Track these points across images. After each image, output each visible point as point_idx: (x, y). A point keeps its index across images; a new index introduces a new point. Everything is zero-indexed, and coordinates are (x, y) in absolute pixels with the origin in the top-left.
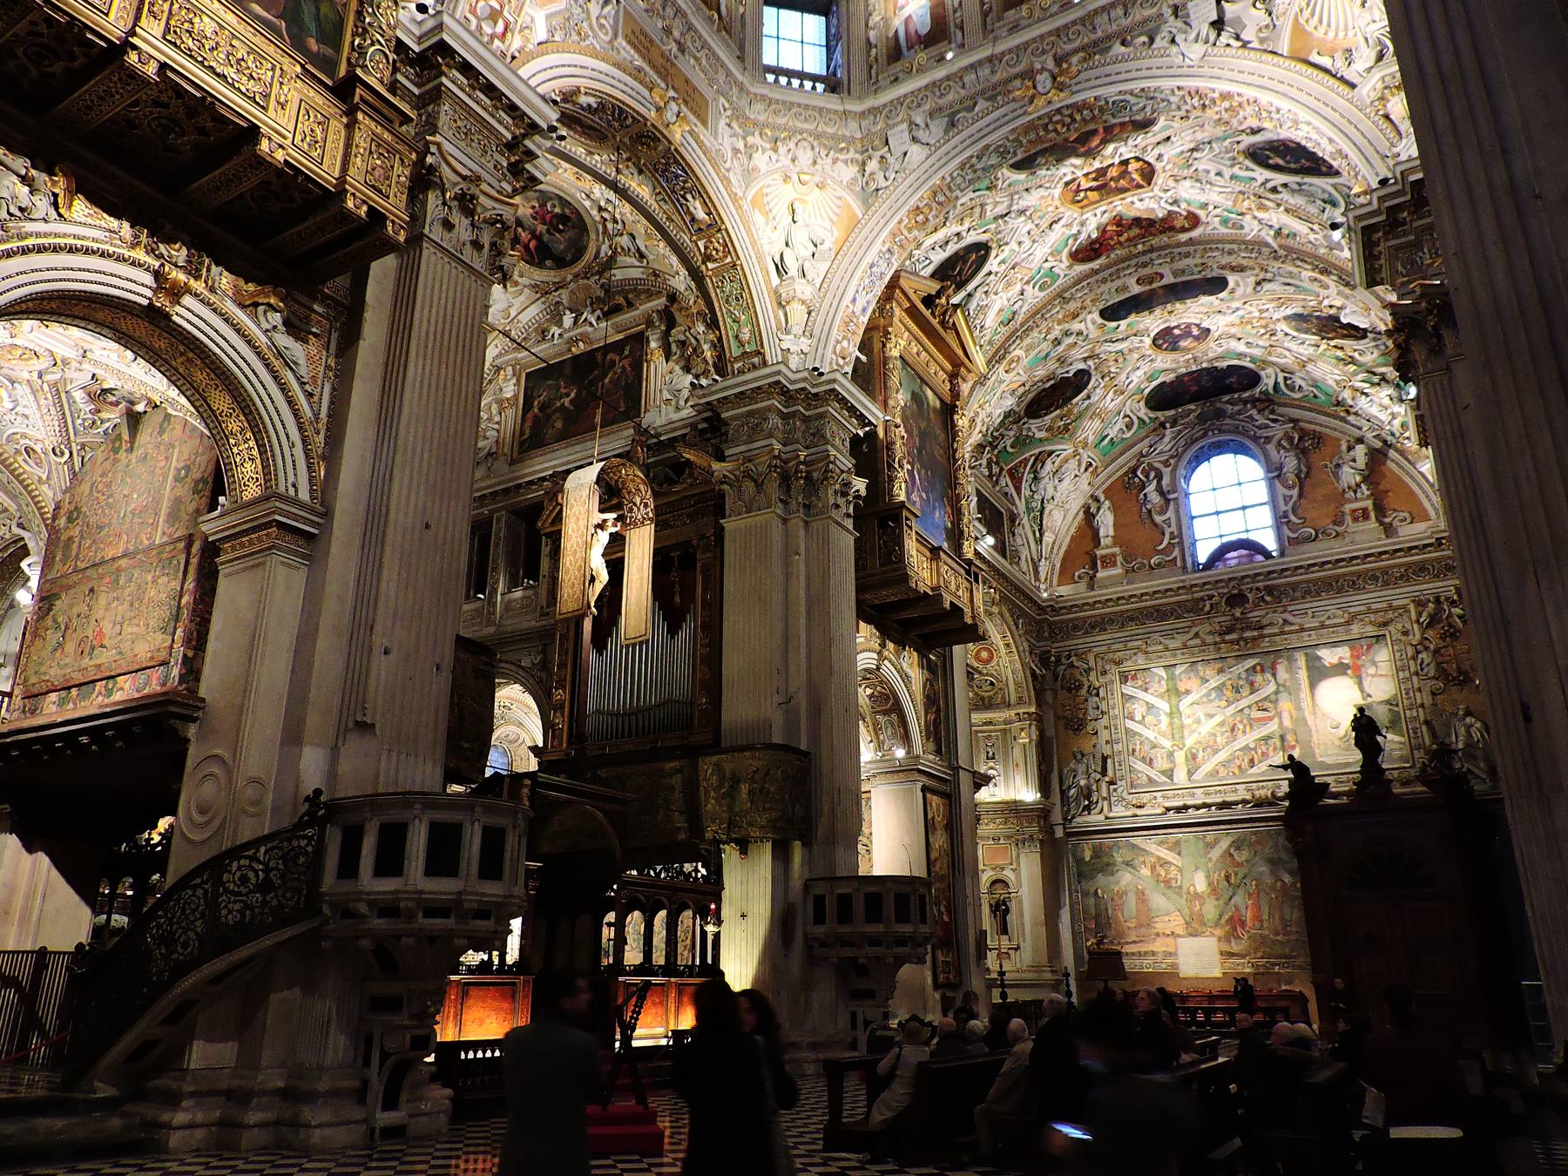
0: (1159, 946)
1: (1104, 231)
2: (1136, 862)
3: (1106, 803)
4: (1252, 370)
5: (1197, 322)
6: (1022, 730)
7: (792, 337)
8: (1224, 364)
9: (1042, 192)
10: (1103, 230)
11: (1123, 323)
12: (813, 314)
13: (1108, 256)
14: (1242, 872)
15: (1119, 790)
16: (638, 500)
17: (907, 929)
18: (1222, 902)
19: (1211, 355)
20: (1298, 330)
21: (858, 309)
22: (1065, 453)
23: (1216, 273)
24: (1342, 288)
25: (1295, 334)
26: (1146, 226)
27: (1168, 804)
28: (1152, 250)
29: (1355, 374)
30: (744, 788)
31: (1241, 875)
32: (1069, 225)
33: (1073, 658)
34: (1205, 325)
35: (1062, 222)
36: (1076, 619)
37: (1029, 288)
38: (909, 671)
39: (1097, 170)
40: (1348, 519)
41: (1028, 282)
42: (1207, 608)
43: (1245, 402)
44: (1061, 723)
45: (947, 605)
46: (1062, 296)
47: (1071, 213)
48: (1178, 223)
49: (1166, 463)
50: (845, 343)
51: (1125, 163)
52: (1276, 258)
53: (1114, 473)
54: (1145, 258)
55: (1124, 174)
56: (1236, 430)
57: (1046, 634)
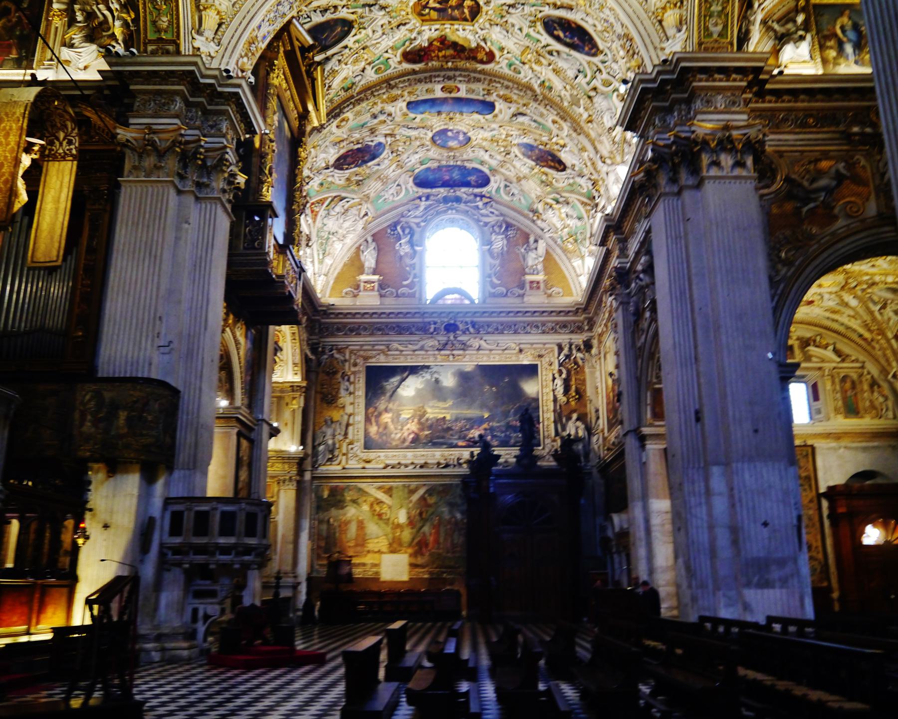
0: (368, 559)
2: (360, 501)
3: (344, 457)
5: (465, 130)
6: (294, 398)
7: (203, 39)
8: (469, 165)
11: (419, 117)
12: (224, 26)
13: (427, 64)
14: (431, 510)
15: (355, 449)
16: (62, 135)
17: (252, 541)
18: (414, 531)
19: (465, 157)
20: (524, 154)
21: (260, 35)
22: (352, 201)
23: (491, 98)
24: (571, 132)
25: (521, 156)
26: (459, 50)
27: (388, 462)
28: (456, 69)
29: (549, 193)
30: (123, 415)
31: (430, 512)
32: (411, 31)
33: (334, 352)
34: (469, 134)
35: (408, 26)
37: (369, 68)
40: (528, 286)
41: (369, 64)
42: (432, 330)
43: (476, 196)
44: (319, 396)
46: (388, 83)
47: (415, 21)
48: (481, 55)
50: (245, 59)
52: (536, 100)
53: (382, 224)
54: (451, 73)
57: (317, 331)
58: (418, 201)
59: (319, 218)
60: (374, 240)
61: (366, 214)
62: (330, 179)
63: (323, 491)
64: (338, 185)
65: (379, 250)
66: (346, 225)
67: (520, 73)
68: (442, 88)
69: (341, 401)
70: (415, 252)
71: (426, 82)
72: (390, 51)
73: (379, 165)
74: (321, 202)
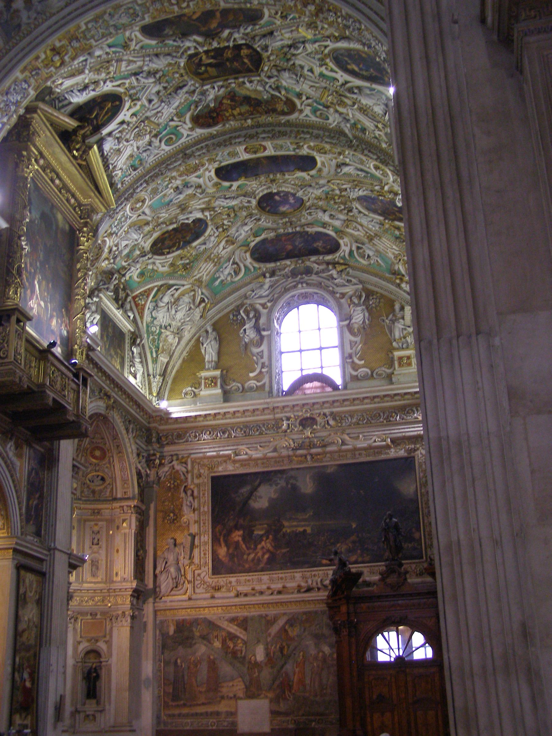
1: (221, 103)
4: (334, 239)
6: (124, 521)
8: (310, 230)
9: (169, 60)
10: (219, 101)
11: (235, 184)
13: (224, 125)
18: (275, 670)
19: (303, 221)
22: (182, 289)
23: (305, 151)
25: (367, 213)
28: (259, 126)
31: (292, 647)
33: (175, 463)
35: (185, 89)
36: (180, 429)
38: (14, 459)
39: (216, 49)
41: (156, 136)
42: (285, 426)
43: (328, 263)
45: (50, 402)
47: (192, 83)
48: (280, 107)
49: (264, 306)
51: (238, 47)
52: (350, 147)
53: (223, 310)
54: (253, 131)
55: (237, 57)
56: (319, 285)
58: (261, 279)
59: (146, 312)
60: (214, 330)
61: (202, 301)
62: (150, 267)
63: (168, 626)
64: (163, 273)
65: (220, 340)
66: (180, 315)
67: (328, 119)
68: (245, 149)
69: (184, 519)
70: (262, 338)
71: (225, 146)
72: (175, 119)
73: (205, 244)
74: (147, 293)
